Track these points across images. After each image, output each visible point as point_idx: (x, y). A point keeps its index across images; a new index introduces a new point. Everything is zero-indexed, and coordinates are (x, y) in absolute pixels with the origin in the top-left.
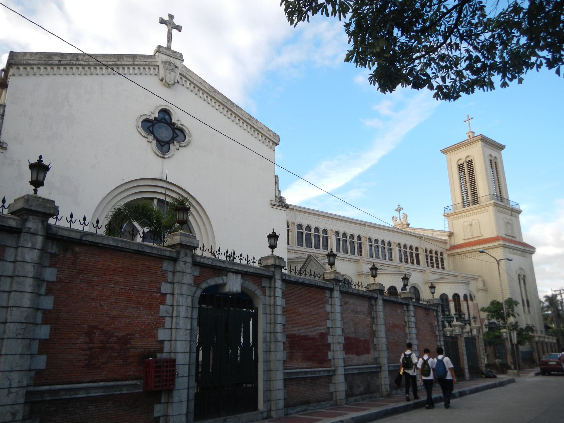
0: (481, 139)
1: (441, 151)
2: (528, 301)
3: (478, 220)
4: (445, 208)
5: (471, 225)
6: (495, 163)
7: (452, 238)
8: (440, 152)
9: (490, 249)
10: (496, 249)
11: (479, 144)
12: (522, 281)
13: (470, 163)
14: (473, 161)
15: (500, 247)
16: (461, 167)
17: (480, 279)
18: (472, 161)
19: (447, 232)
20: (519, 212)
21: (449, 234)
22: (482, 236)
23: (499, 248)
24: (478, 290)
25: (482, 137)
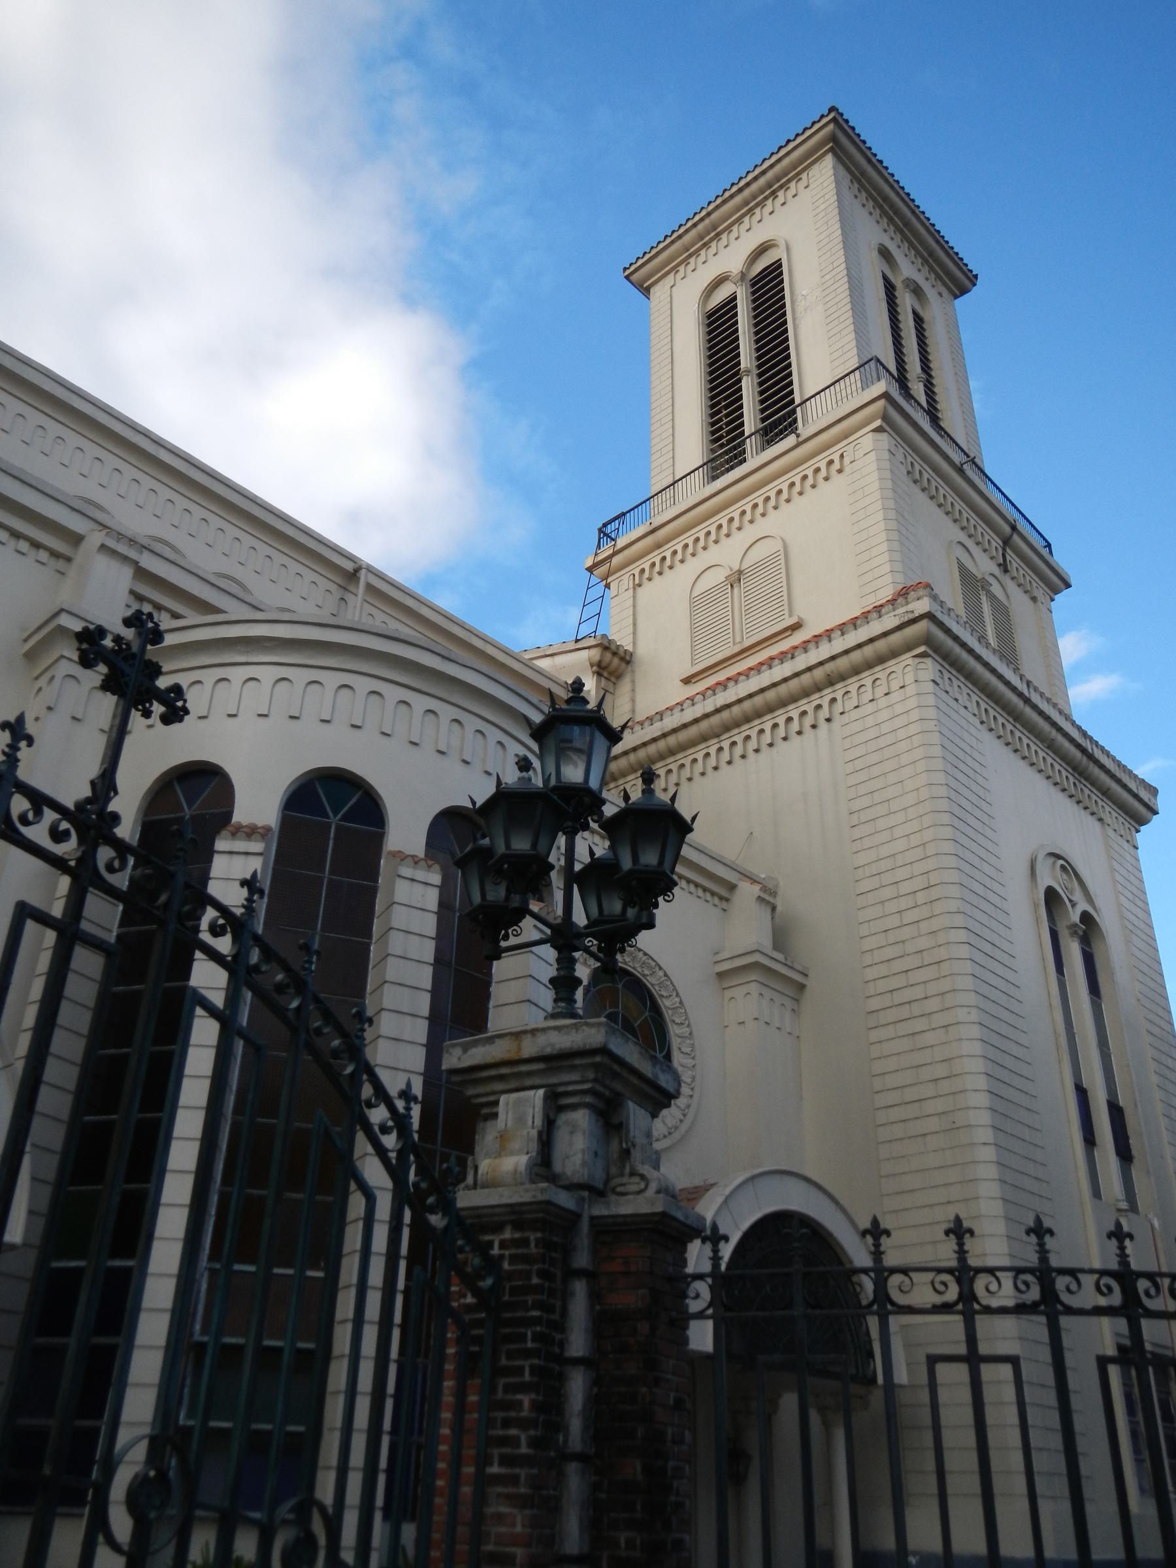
0: (833, 138)
1: (625, 269)
2: (1116, 1112)
3: (783, 540)
5: (736, 578)
7: (625, 687)
8: (622, 275)
9: (843, 677)
10: (880, 672)
11: (824, 173)
12: (1073, 951)
15: (908, 647)
17: (747, 892)
18: (780, 266)
19: (591, 642)
20: (1057, 582)
21: (595, 654)
22: (796, 627)
23: (907, 658)
24: (721, 975)
25: (834, 120)
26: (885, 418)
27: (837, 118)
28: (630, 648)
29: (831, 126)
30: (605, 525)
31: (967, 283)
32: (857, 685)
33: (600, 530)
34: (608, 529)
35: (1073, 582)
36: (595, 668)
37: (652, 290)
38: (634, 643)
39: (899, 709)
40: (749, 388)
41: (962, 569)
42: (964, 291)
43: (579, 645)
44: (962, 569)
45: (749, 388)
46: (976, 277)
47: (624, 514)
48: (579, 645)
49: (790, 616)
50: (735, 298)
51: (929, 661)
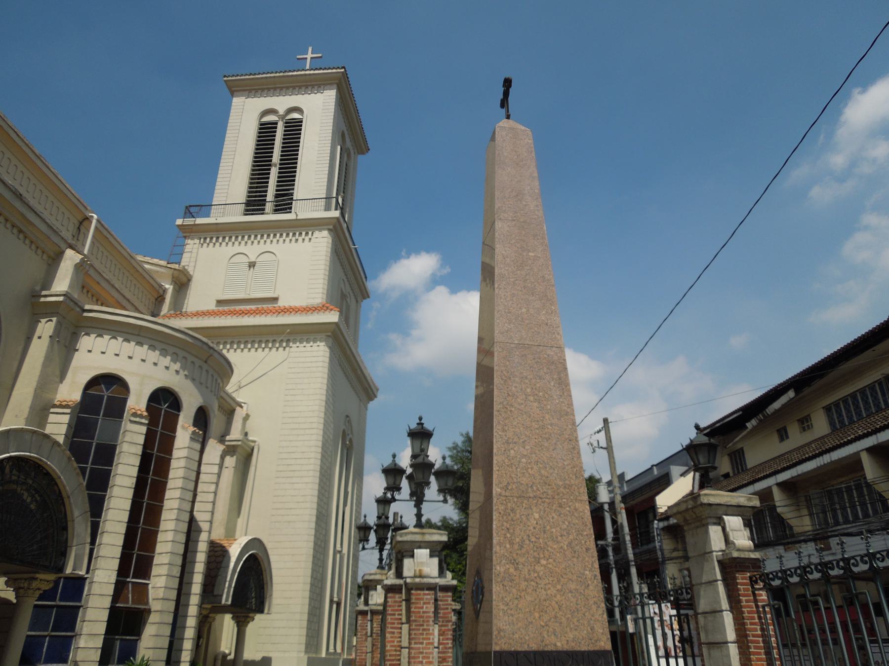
4: (187, 207)
5: (252, 265)
6: (346, 165)
13: (294, 129)
14: (304, 124)
16: (266, 132)
18: (302, 122)
26: (335, 227)
27: (345, 75)
28: (191, 273)
29: (341, 74)
30: (190, 206)
31: (365, 150)
32: (300, 338)
33: (187, 207)
34: (192, 210)
35: (370, 296)
36: (174, 279)
37: (235, 93)
38: (194, 271)
39: (315, 354)
40: (274, 173)
41: (342, 291)
42: (363, 153)
43: (169, 266)
44: (342, 291)
45: (274, 173)
46: (369, 150)
47: (202, 206)
48: (169, 266)
49: (274, 292)
50: (276, 123)
51: (330, 339)
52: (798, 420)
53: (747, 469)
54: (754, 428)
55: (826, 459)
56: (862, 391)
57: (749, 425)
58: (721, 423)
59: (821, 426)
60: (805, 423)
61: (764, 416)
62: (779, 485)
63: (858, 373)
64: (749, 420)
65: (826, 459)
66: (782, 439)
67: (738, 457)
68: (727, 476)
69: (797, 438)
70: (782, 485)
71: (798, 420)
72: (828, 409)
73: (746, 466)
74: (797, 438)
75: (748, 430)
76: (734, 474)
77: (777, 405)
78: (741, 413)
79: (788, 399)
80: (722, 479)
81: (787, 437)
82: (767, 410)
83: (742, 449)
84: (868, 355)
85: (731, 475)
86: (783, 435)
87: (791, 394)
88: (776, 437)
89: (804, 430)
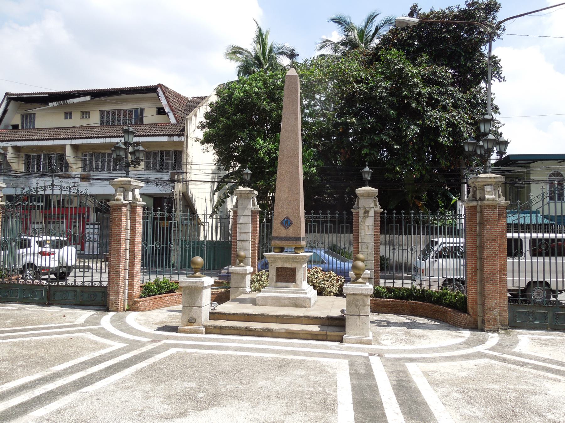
52: (81, 112)
53: (34, 128)
54: (54, 107)
55: (108, 140)
56: (125, 111)
57: (51, 104)
58: (29, 96)
59: (95, 119)
60: (85, 114)
61: (64, 103)
62: (71, 145)
63: (126, 101)
64: (52, 101)
65: (108, 140)
66: (66, 118)
67: (28, 118)
68: (15, 127)
69: (76, 120)
70: (75, 148)
71: (81, 112)
72: (102, 112)
73: (34, 125)
74: (76, 120)
75: (48, 107)
76: (22, 128)
77: (76, 100)
78: (48, 95)
79: (85, 100)
80: (11, 128)
81: (71, 118)
82: (68, 101)
83: (34, 114)
84: (138, 96)
85: (20, 128)
86: (68, 115)
87: (88, 98)
88: (63, 116)
89: (83, 117)
